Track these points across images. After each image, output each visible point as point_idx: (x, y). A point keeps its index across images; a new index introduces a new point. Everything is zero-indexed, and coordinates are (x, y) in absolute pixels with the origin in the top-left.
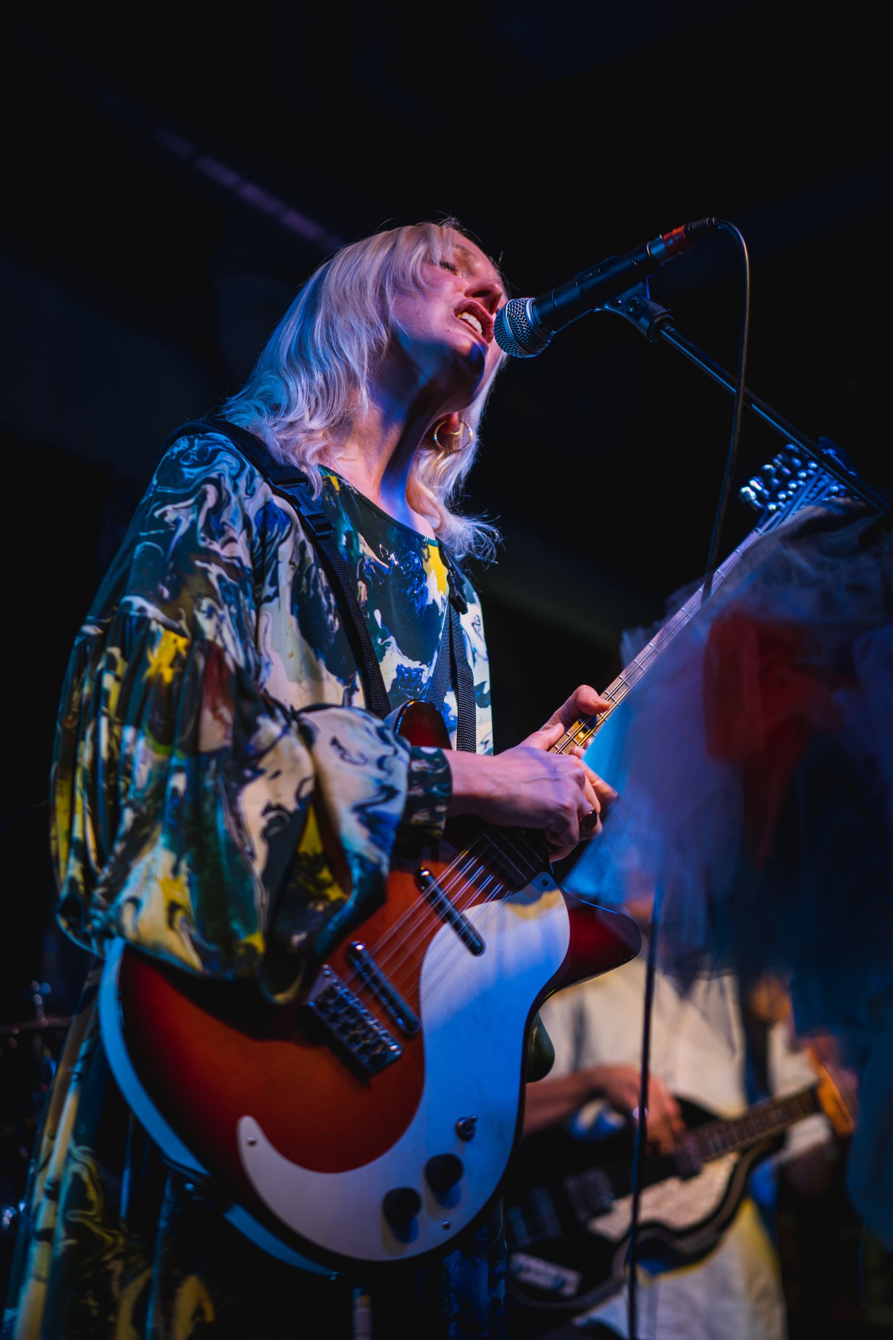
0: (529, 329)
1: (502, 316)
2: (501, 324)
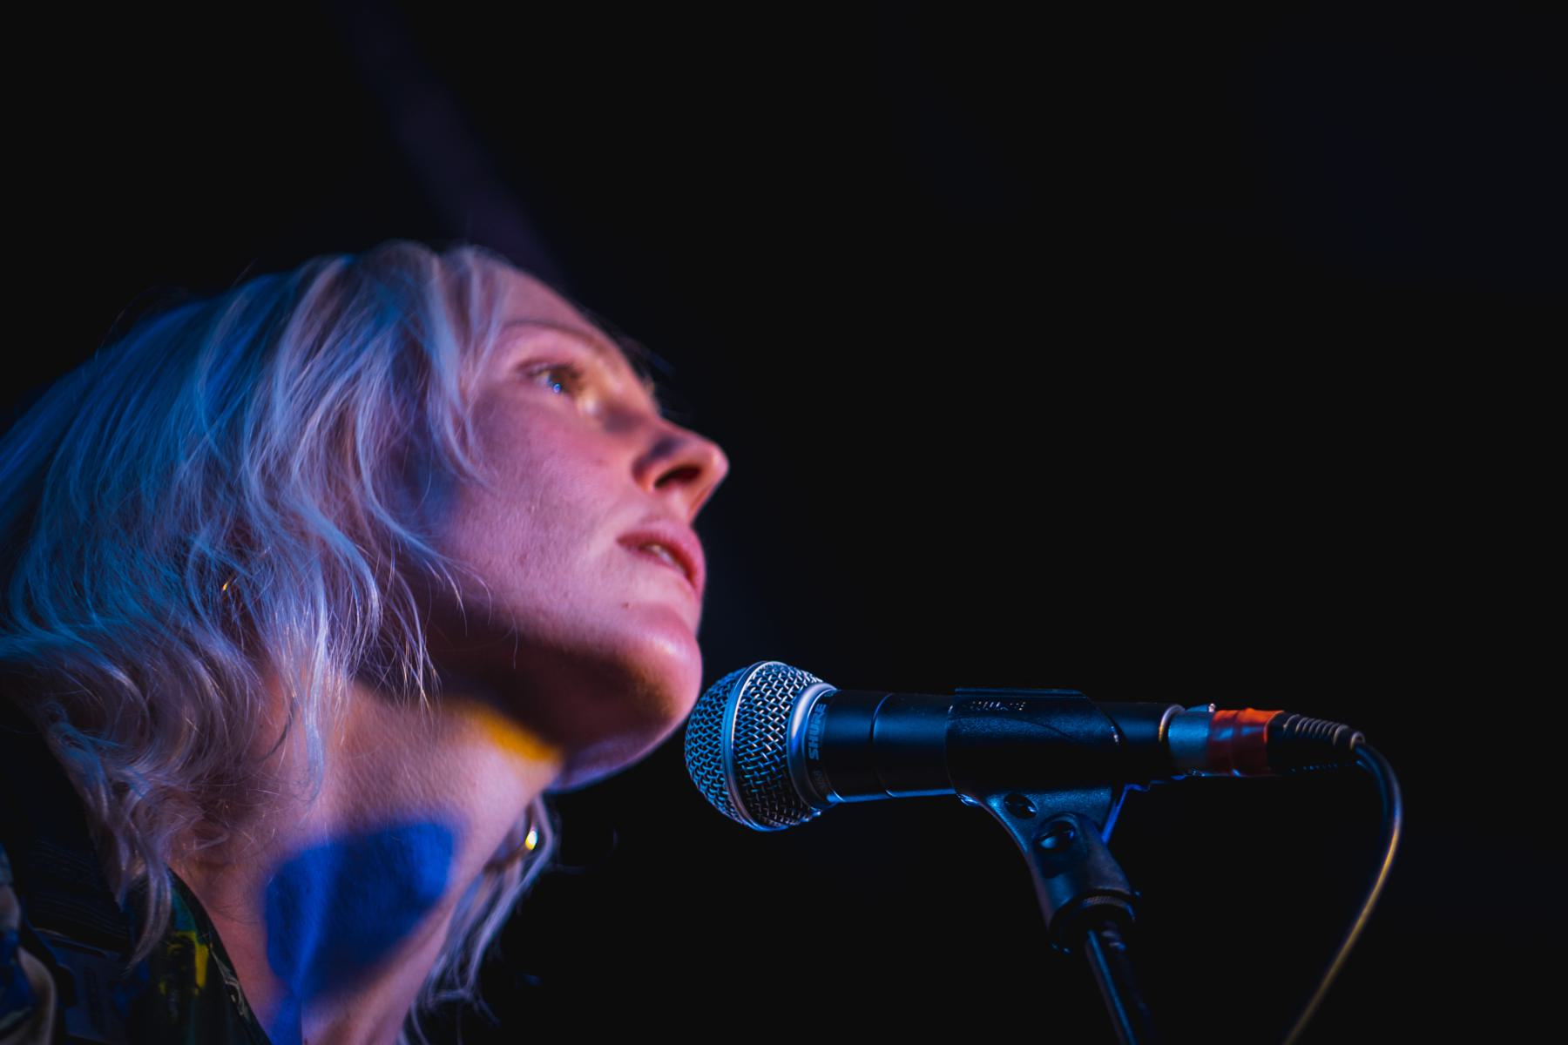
0: (779, 753)
1: (732, 687)
2: (719, 705)
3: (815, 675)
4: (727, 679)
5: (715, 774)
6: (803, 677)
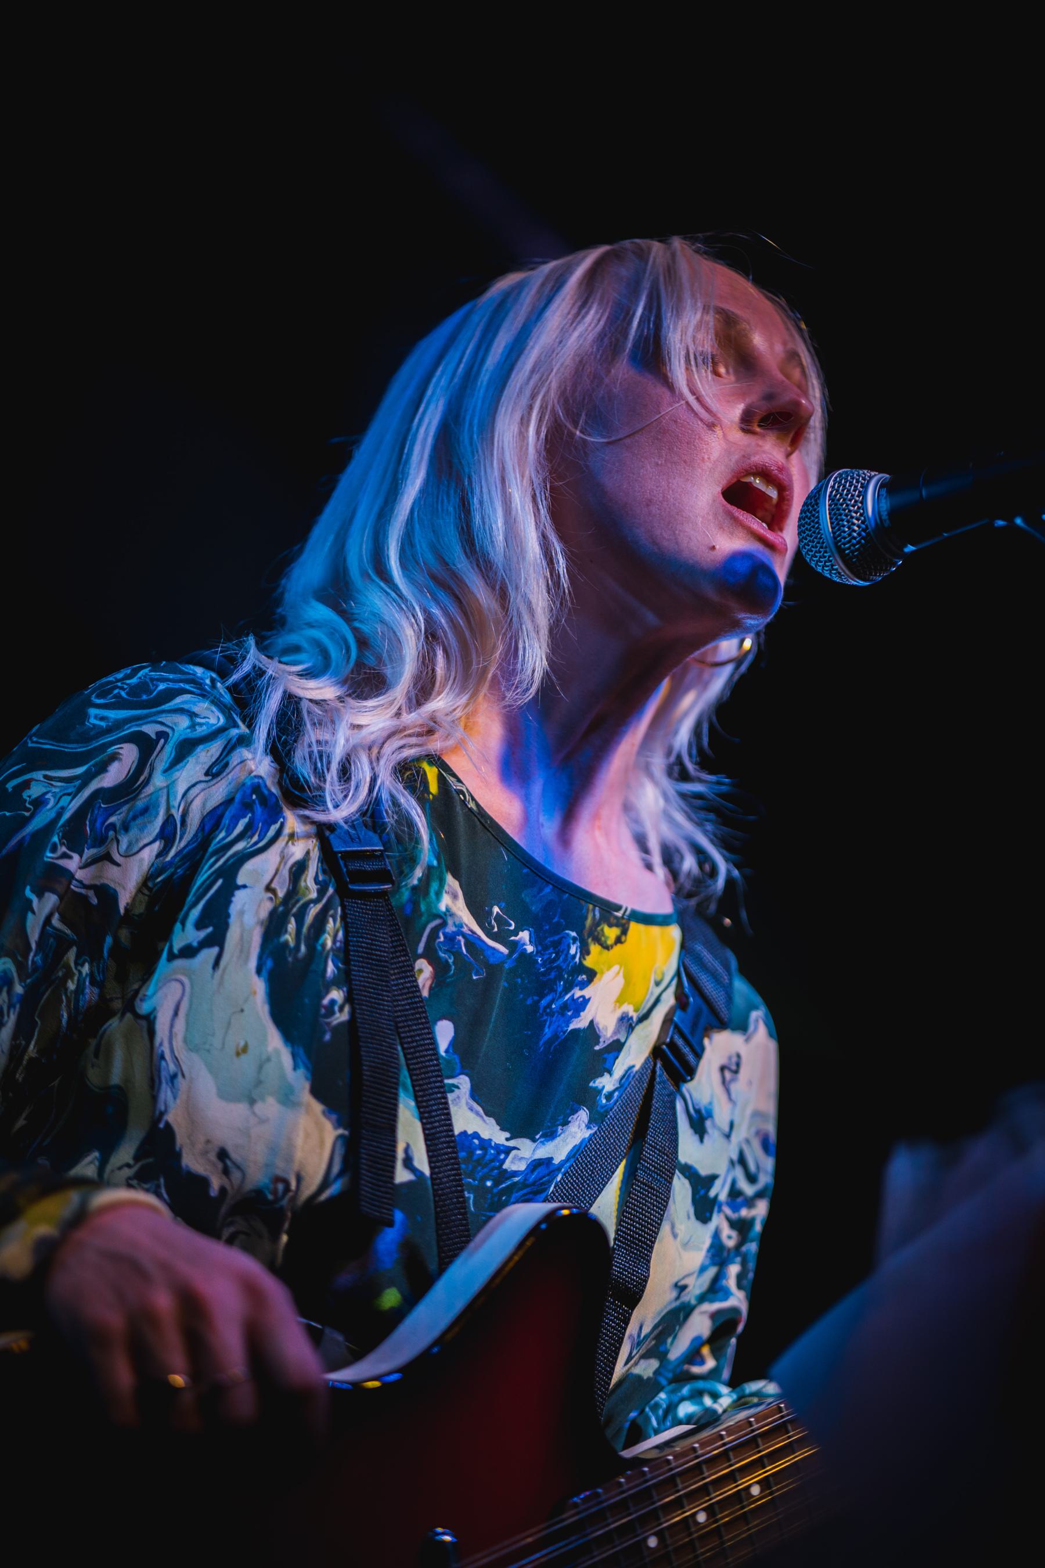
0: (863, 530)
1: (819, 495)
2: (815, 510)
3: (872, 470)
6: (864, 473)
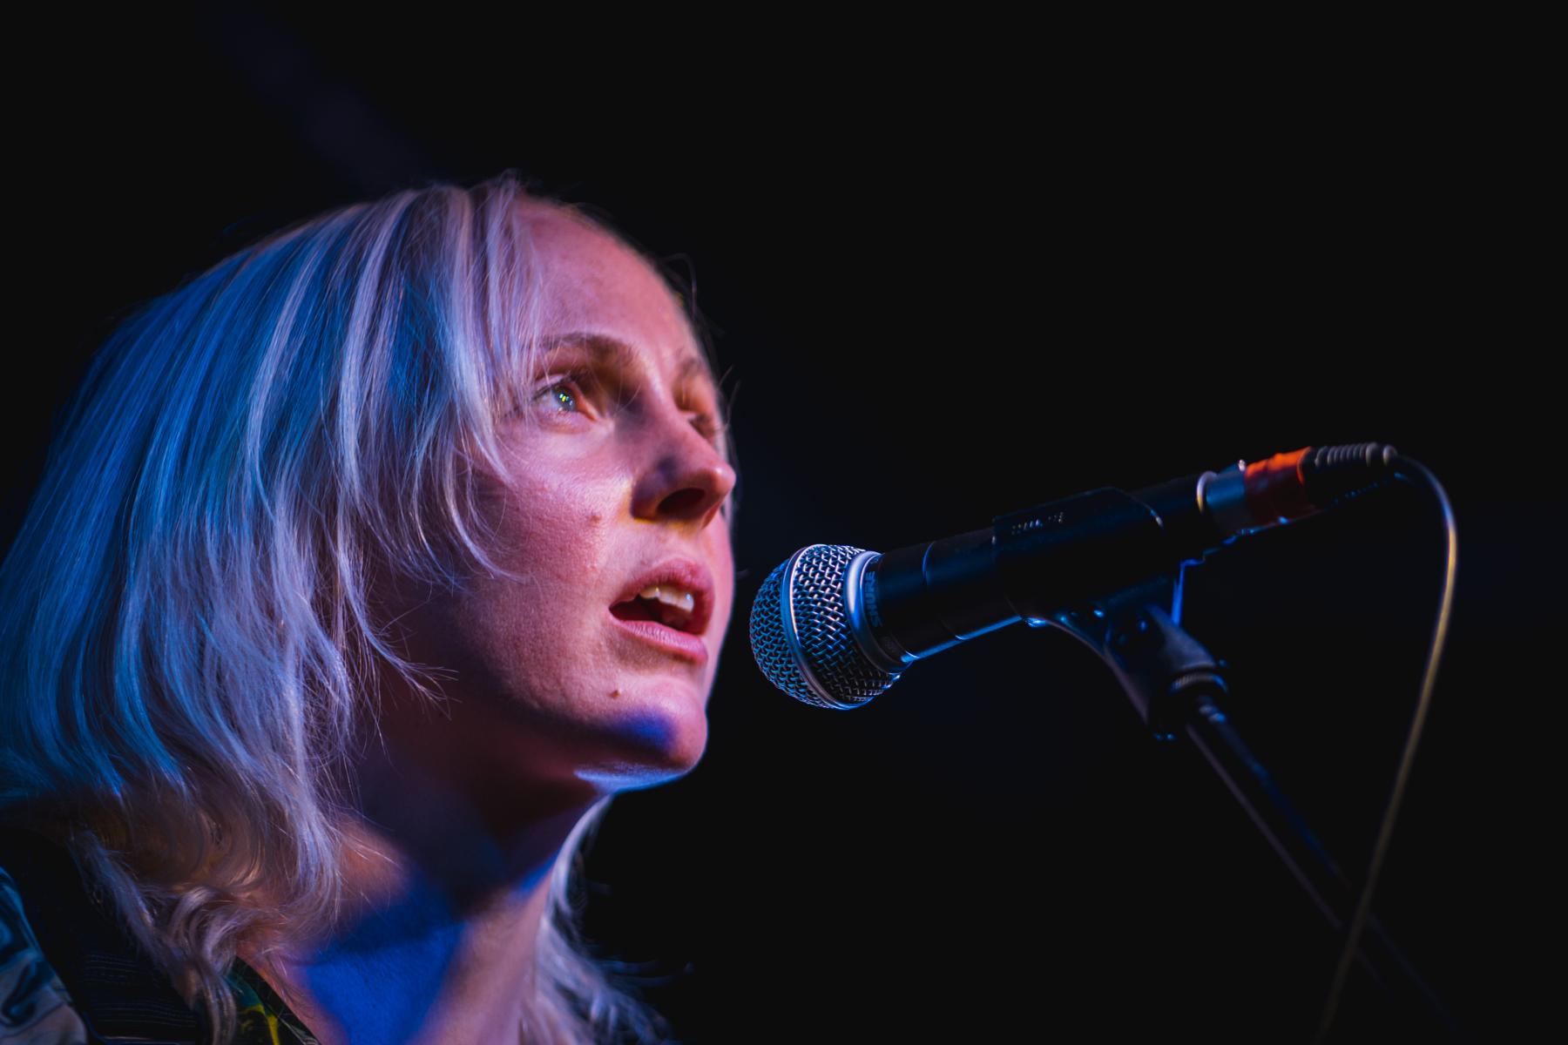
0: (843, 631)
1: (781, 581)
2: (774, 602)
3: (856, 547)
4: (774, 575)
5: (788, 669)
6: (845, 552)
